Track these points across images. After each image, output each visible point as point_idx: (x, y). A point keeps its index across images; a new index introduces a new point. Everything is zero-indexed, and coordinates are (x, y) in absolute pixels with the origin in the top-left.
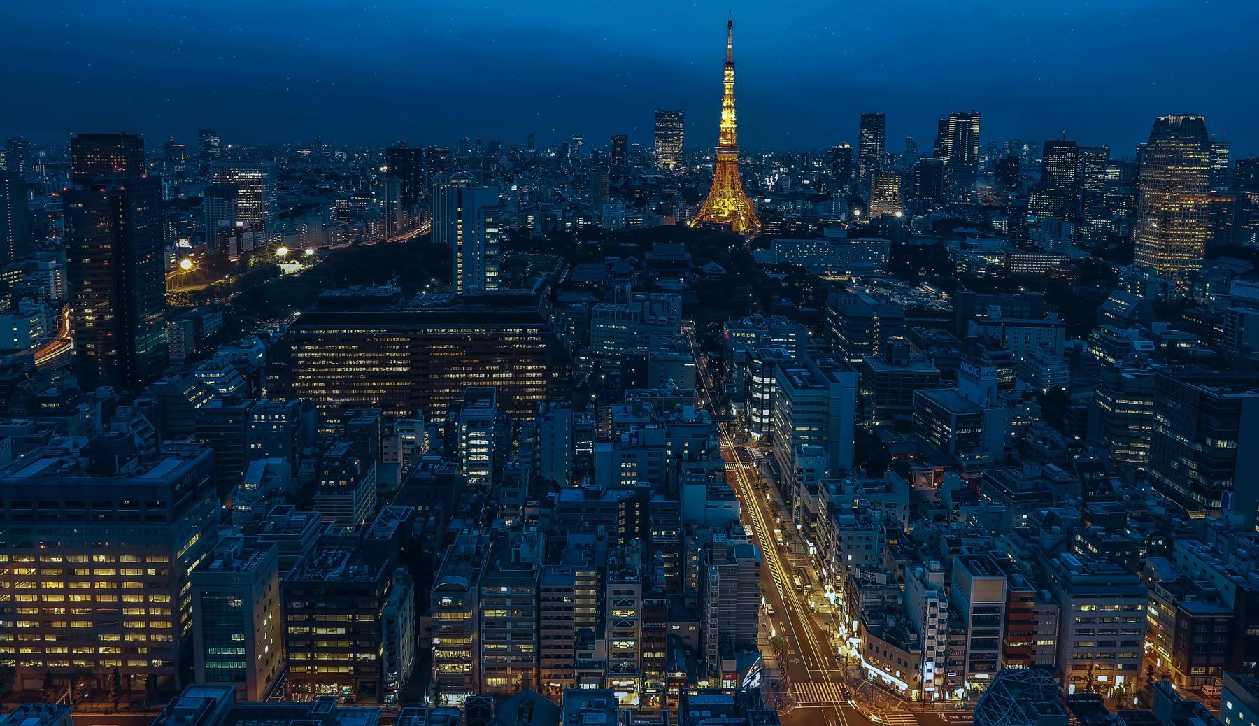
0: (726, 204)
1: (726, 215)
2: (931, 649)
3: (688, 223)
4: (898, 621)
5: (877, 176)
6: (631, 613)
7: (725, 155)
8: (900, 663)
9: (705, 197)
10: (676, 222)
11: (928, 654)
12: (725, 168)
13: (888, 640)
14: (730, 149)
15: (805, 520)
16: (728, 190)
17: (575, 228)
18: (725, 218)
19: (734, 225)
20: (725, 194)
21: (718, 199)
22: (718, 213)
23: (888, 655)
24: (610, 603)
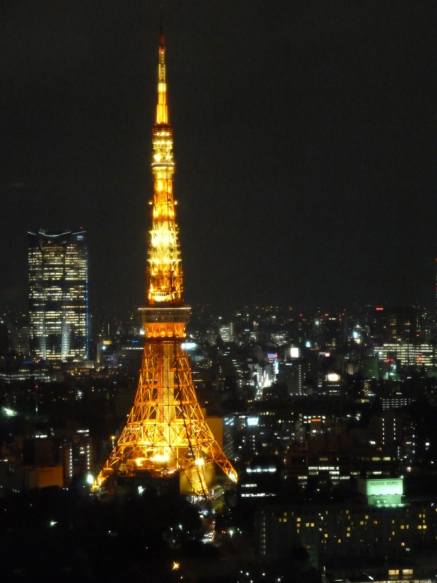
0: (166, 435)
7: (162, 325)
12: (160, 352)
18: (165, 466)
19: (183, 479)
20: (162, 412)
21: (148, 423)
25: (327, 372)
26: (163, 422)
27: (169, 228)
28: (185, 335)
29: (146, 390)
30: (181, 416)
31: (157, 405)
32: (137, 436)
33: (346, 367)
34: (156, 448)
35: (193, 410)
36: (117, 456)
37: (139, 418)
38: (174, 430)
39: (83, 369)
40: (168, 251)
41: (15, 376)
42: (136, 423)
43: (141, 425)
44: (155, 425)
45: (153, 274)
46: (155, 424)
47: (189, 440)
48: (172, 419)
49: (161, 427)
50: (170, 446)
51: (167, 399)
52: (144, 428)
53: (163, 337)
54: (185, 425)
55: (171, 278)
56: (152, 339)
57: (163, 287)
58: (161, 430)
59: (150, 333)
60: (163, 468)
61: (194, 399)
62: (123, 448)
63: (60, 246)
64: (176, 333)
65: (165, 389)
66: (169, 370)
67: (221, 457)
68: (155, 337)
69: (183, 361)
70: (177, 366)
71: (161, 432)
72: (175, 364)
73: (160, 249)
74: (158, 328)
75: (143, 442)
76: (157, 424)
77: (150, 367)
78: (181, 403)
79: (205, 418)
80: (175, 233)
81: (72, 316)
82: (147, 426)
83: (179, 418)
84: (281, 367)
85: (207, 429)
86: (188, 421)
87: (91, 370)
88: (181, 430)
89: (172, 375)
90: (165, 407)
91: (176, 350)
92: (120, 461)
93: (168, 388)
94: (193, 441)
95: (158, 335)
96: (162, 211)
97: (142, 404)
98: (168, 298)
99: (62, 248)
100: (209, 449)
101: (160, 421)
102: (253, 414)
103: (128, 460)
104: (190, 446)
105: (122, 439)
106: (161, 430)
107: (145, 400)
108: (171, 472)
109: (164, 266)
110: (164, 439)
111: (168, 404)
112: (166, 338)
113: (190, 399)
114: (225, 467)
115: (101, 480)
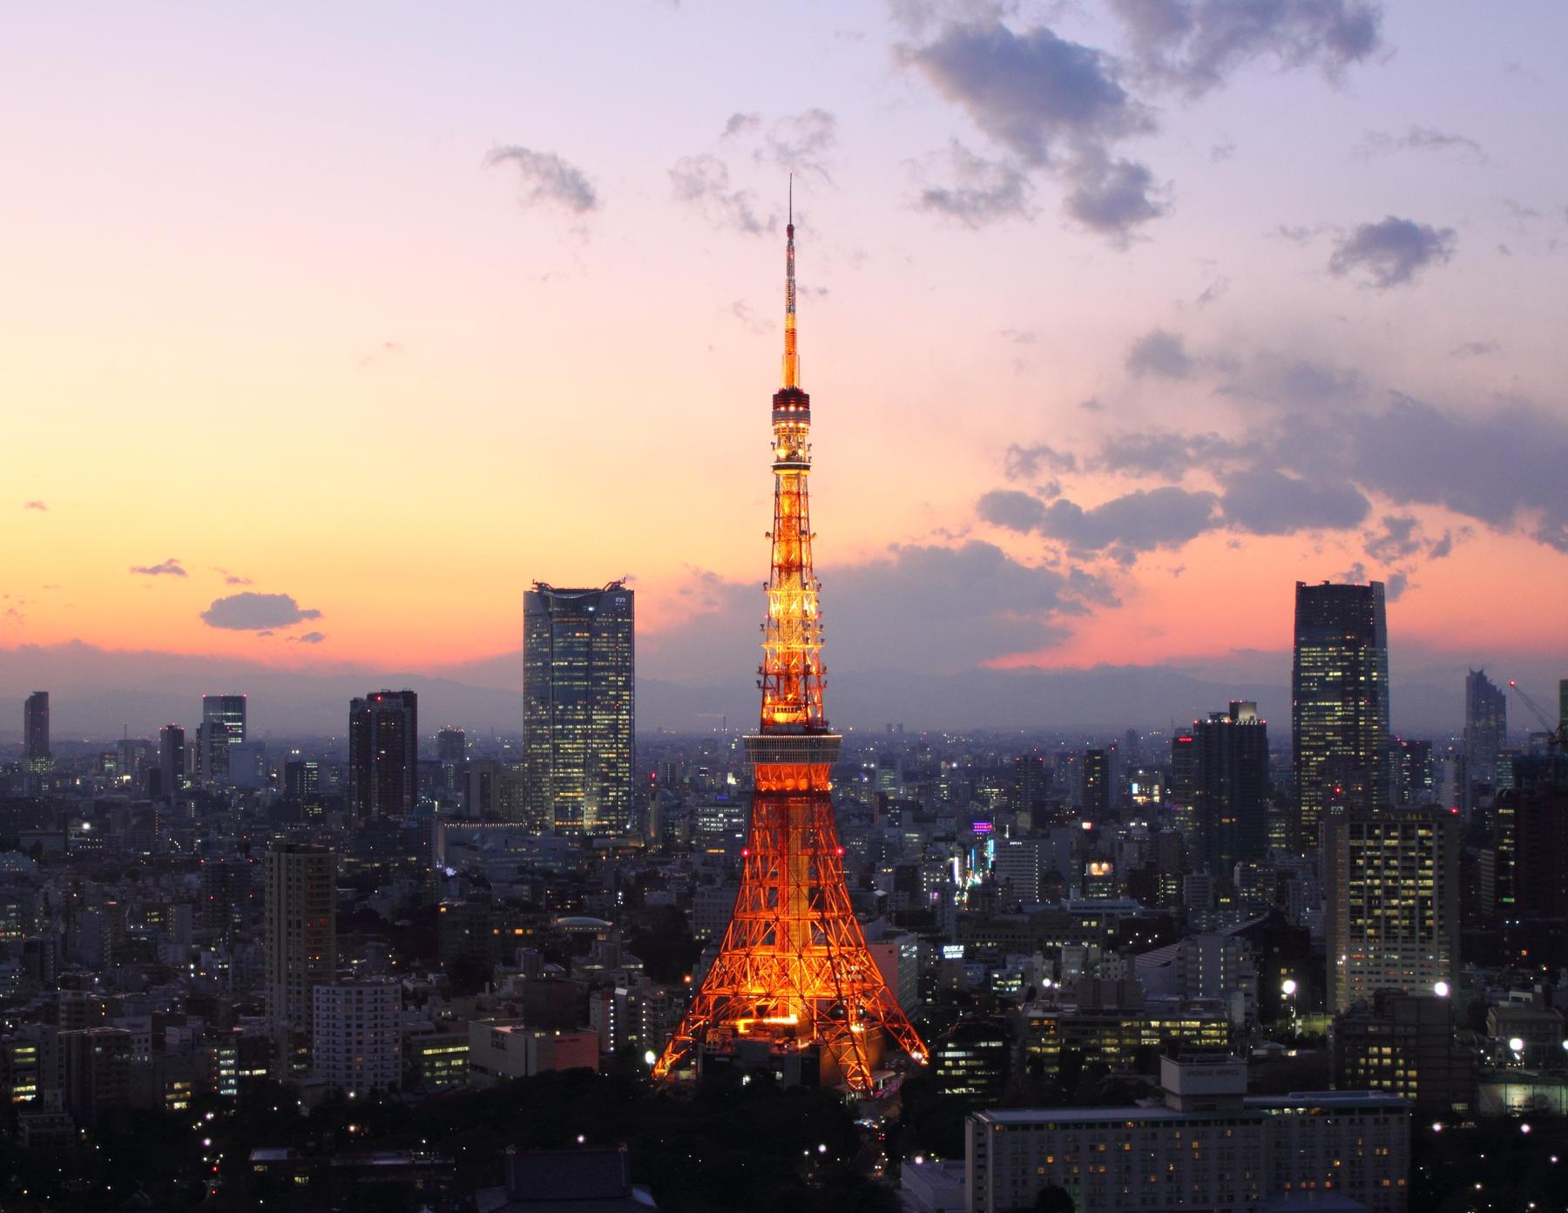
1: (792, 1020)
3: (650, 1057)
5: (1356, 833)
7: (787, 768)
9: (715, 945)
16: (799, 916)
18: (790, 1032)
19: (826, 1058)
20: (786, 931)
21: (761, 953)
22: (762, 1011)
26: (788, 951)
27: (804, 586)
29: (756, 889)
31: (777, 919)
32: (738, 976)
34: (774, 1000)
35: (844, 928)
36: (702, 1014)
38: (810, 966)
39: (623, 848)
40: (800, 628)
41: (498, 860)
42: (736, 952)
43: (747, 955)
44: (773, 956)
46: (772, 954)
47: (837, 985)
48: (805, 945)
49: (784, 960)
50: (802, 997)
51: (796, 908)
52: (751, 961)
53: (788, 789)
54: (829, 958)
56: (769, 792)
58: (784, 966)
59: (764, 783)
60: (787, 1038)
61: (846, 909)
62: (712, 1000)
63: (583, 617)
64: (813, 783)
65: (792, 889)
66: (799, 853)
67: (896, 1019)
68: (774, 789)
71: (783, 969)
73: (786, 622)
74: (780, 773)
75: (753, 988)
76: (776, 954)
77: (764, 845)
78: (823, 915)
79: (866, 944)
81: (604, 748)
82: (758, 958)
83: (818, 943)
85: (871, 966)
86: (835, 952)
88: (821, 966)
90: (792, 922)
93: (798, 886)
95: (779, 786)
96: (789, 553)
97: (748, 916)
98: (800, 715)
99: (587, 620)
100: (874, 1002)
101: (783, 949)
103: (722, 1022)
104: (840, 996)
105: (711, 982)
106: (784, 966)
107: (752, 910)
108: (802, 1045)
109: (791, 655)
110: (791, 983)
111: (797, 917)
112: (796, 792)
113: (840, 909)
114: (903, 1038)
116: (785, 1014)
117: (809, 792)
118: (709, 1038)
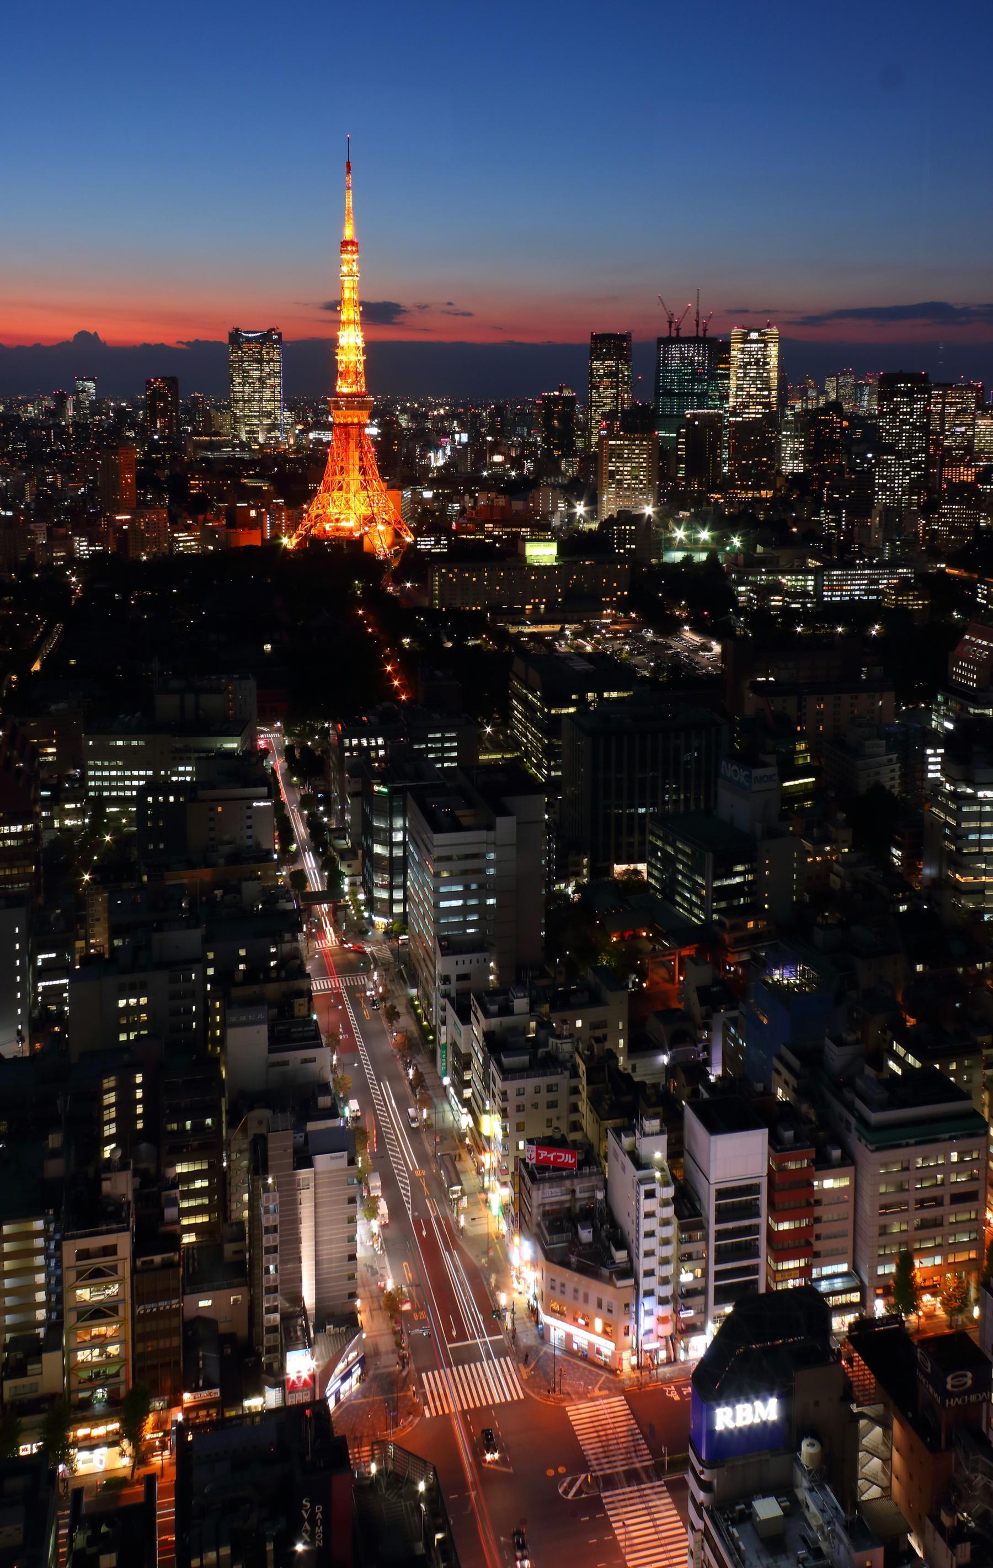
2: (650, 1273)
4: (596, 1233)
6: (114, 1289)
7: (349, 412)
8: (600, 1305)
10: (264, 540)
11: (645, 1284)
12: (348, 435)
13: (582, 1270)
14: (353, 401)
15: (455, 1068)
16: (354, 478)
17: (72, 560)
18: (351, 531)
19: (366, 540)
20: (348, 485)
21: (336, 494)
23: (581, 1295)
24: (70, 1276)
25: (492, 454)
28: (368, 421)
30: (365, 488)
33: (509, 450)
37: (327, 490)
38: (359, 501)
45: (341, 369)
55: (357, 373)
56: (340, 424)
57: (349, 381)
62: (313, 516)
69: (368, 444)
70: (362, 447)
72: (360, 446)
75: (332, 510)
80: (361, 334)
84: (452, 450)
86: (371, 494)
87: (285, 450)
89: (357, 454)
91: (361, 435)
92: (311, 527)
94: (375, 510)
97: (330, 479)
101: (346, 493)
102: (429, 488)
110: (349, 508)
115: (295, 541)
116: (347, 520)
117: (359, 424)
118: (313, 531)
